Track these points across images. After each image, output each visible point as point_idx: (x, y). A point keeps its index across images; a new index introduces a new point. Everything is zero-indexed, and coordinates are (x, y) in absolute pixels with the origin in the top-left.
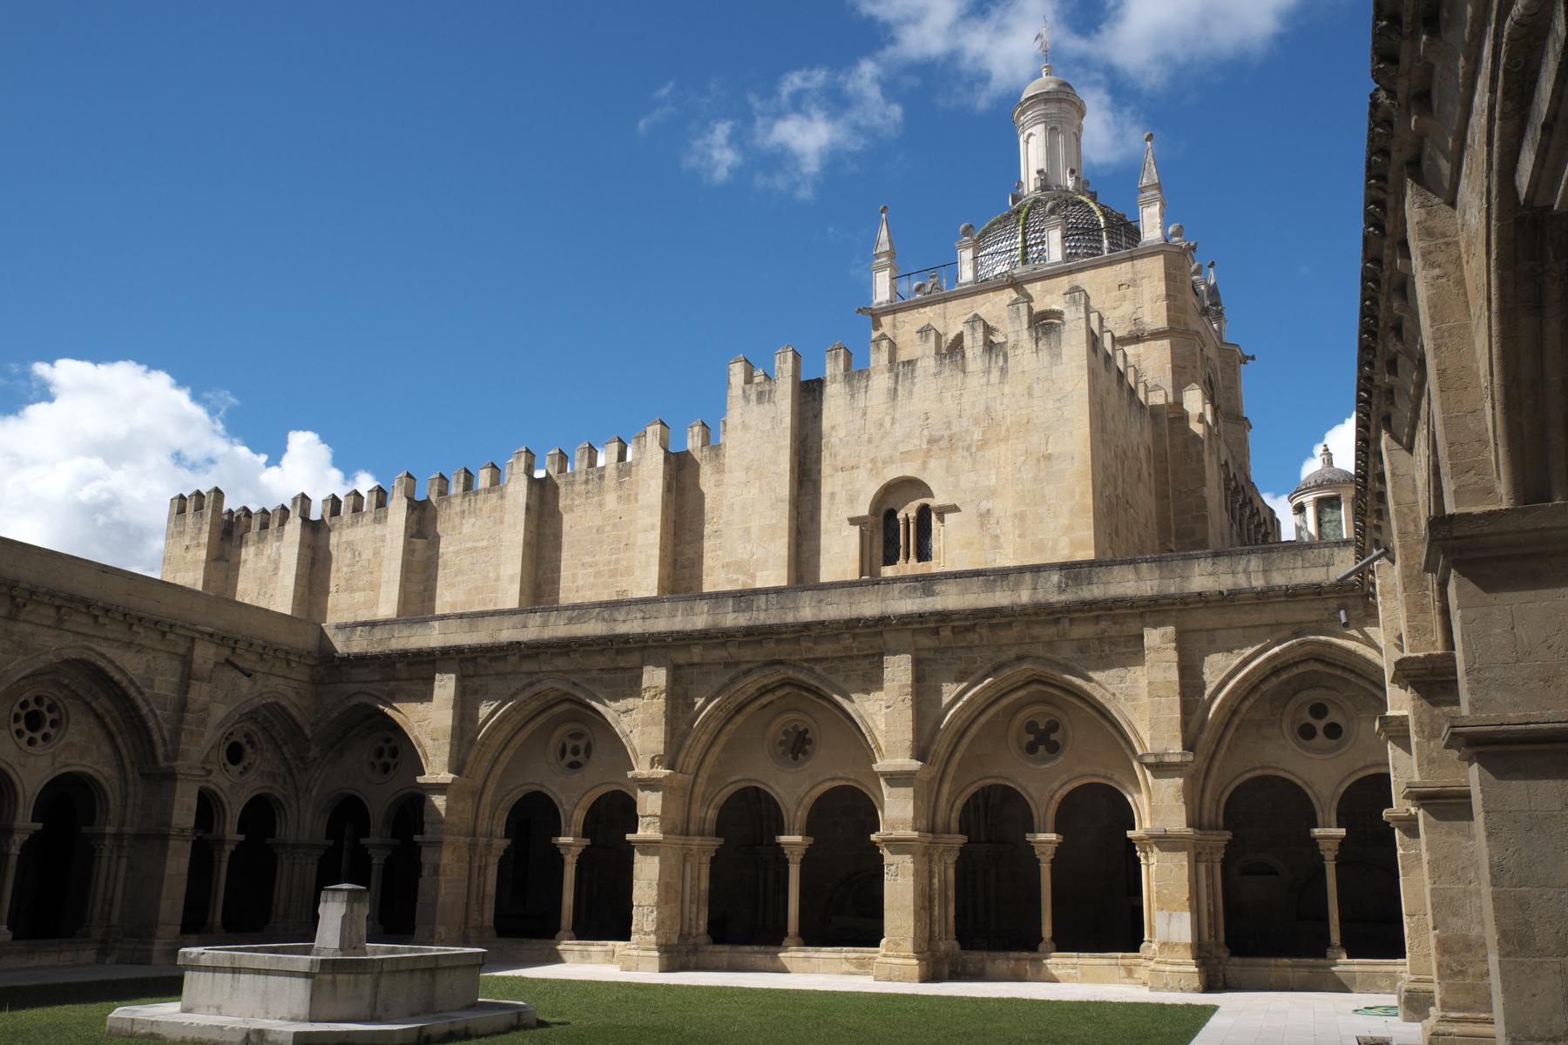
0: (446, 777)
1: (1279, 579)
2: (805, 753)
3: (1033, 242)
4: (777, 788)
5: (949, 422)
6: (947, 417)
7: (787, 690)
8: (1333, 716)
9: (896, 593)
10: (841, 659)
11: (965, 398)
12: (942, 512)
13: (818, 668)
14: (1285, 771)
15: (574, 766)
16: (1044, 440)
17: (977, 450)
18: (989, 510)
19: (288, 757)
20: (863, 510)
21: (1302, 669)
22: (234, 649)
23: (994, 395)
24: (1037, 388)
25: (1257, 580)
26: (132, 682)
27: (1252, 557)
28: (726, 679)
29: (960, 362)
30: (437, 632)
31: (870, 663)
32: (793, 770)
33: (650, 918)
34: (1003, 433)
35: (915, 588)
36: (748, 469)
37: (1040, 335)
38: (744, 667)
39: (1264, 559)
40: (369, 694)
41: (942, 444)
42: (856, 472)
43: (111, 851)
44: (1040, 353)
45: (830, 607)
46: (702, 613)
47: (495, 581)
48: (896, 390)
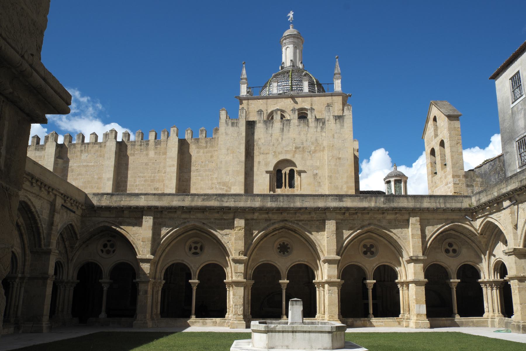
0: (149, 256)
1: (448, 206)
2: (280, 252)
3: (294, 84)
4: (279, 264)
5: (303, 142)
6: (302, 140)
7: (283, 230)
8: (455, 247)
9: (330, 200)
10: (309, 221)
11: (308, 135)
12: (300, 173)
13: (300, 223)
14: (443, 262)
15: (195, 254)
16: (338, 153)
17: (313, 153)
18: (317, 174)
19: (67, 246)
20: (271, 169)
21: (449, 232)
22: (65, 201)
23: (319, 135)
24: (336, 136)
25: (442, 205)
26: (37, 212)
27: (441, 198)
28: (266, 225)
29: (307, 123)
30: (143, 200)
31: (319, 223)
32: (285, 258)
33: (240, 309)
34: (322, 148)
35: (336, 199)
36: (228, 149)
37: (337, 118)
38: (272, 221)
39: (444, 199)
40: (109, 222)
41: (300, 149)
42: (268, 155)
43: (18, 284)
44: (337, 124)
45: (307, 203)
46: (258, 201)
47: (97, 179)
48: (283, 129)
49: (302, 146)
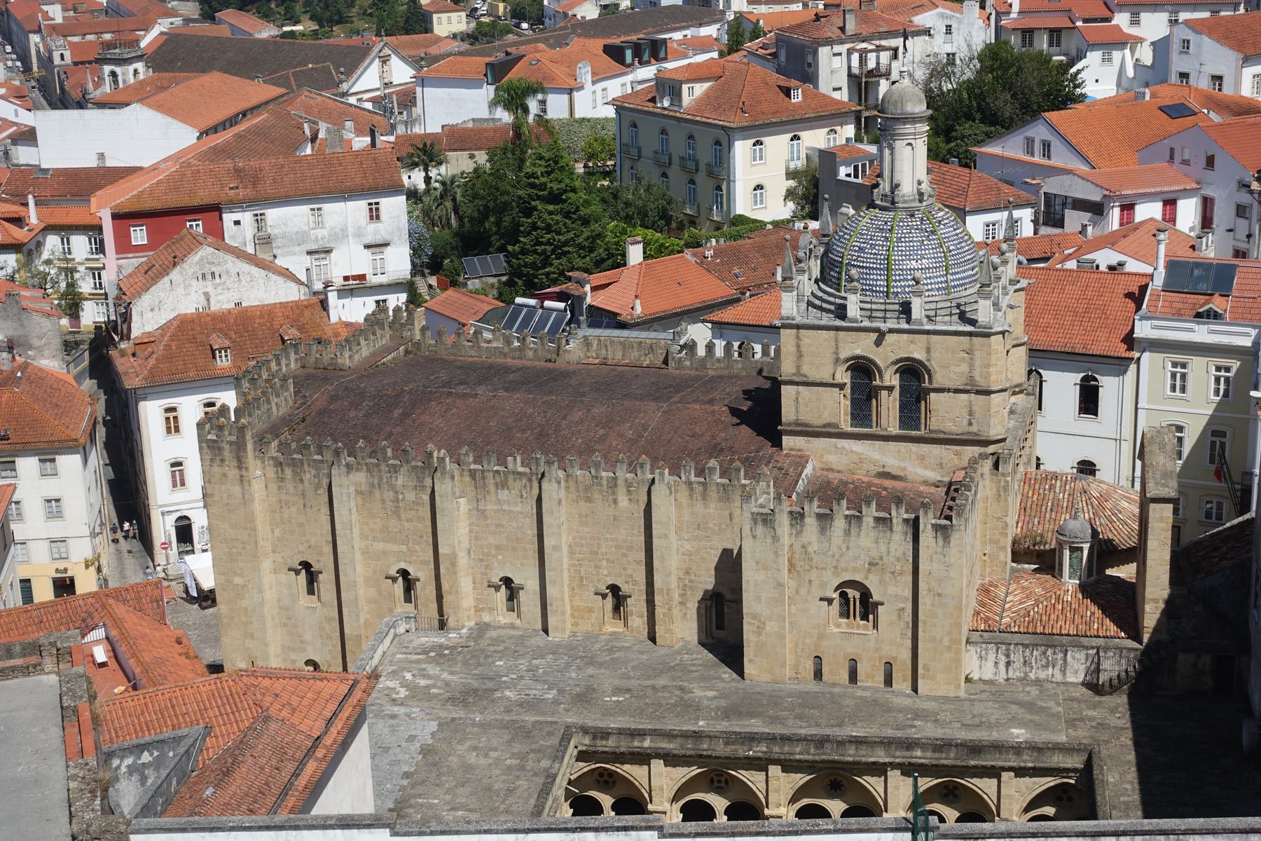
36: (758, 563)
42: (824, 572)
48: (849, 530)
49: (880, 562)
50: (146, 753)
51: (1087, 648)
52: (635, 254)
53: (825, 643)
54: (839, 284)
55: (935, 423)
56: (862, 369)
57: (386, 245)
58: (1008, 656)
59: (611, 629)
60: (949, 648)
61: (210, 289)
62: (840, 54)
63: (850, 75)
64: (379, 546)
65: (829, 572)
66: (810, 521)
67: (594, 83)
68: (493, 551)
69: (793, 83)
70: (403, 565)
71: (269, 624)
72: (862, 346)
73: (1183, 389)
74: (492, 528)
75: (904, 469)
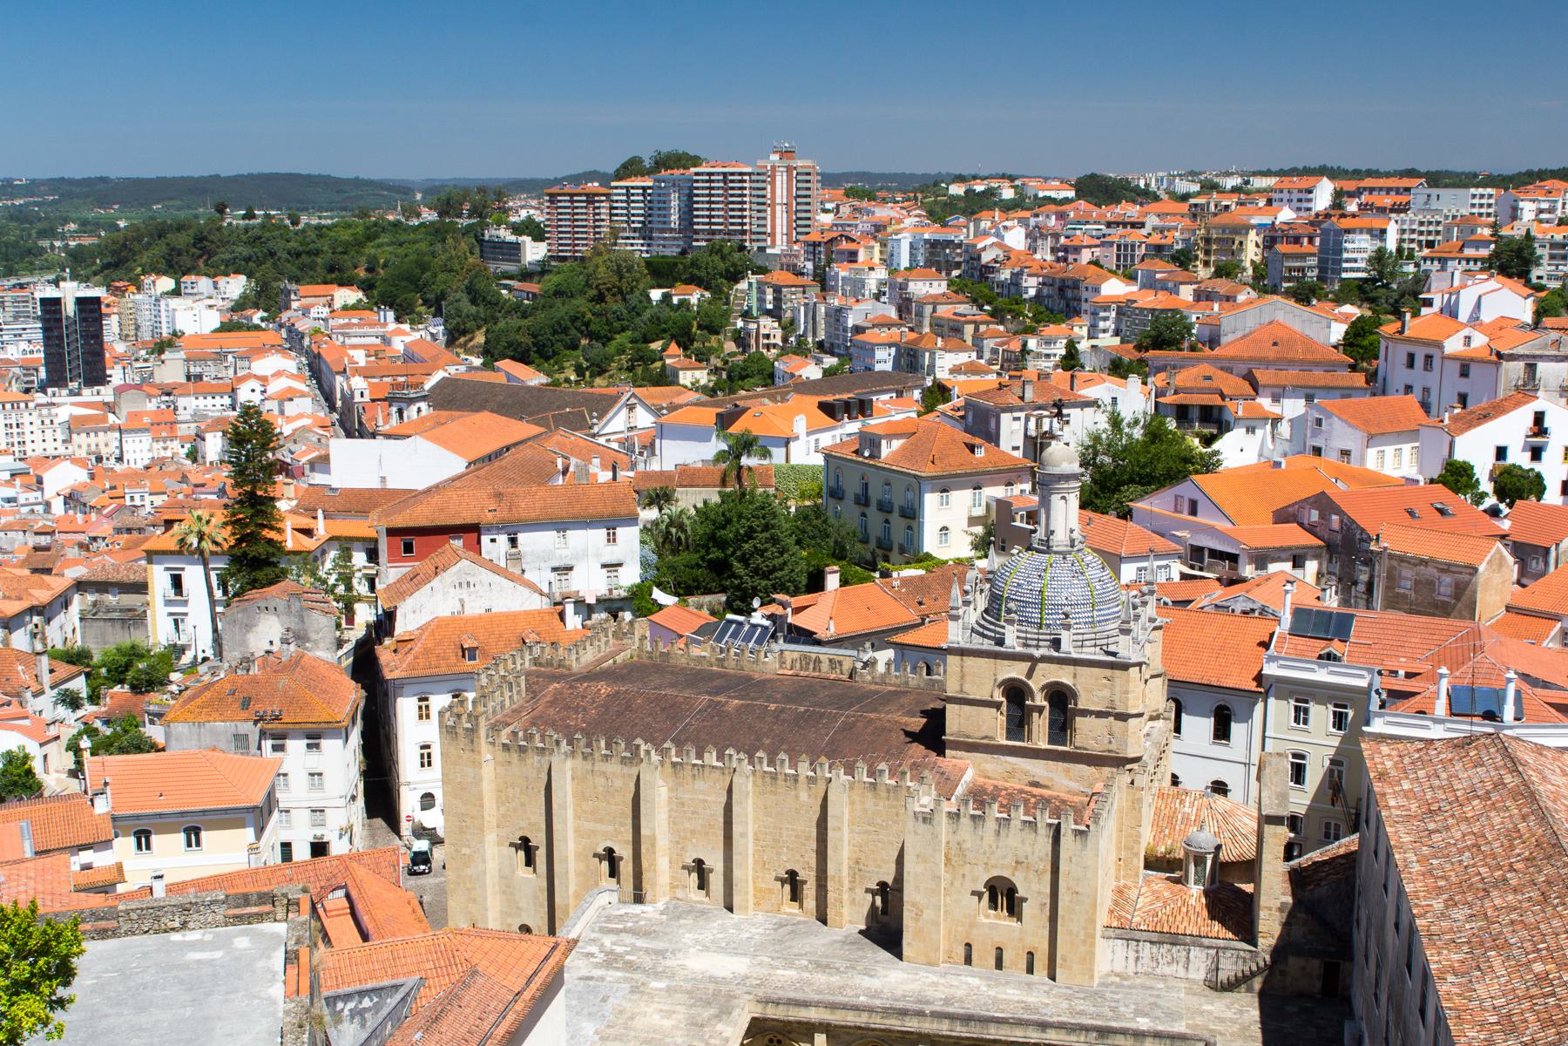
24: (1074, 860)
36: (918, 856)
50: (367, 999)
51: (1208, 947)
52: (832, 581)
53: (975, 931)
54: (1000, 615)
55: (1079, 740)
56: (1016, 693)
57: (620, 565)
58: (1137, 952)
59: (788, 910)
60: (1084, 942)
61: (465, 597)
62: (1019, 419)
63: (1026, 435)
64: (591, 825)
65: (980, 868)
66: (965, 821)
67: (808, 434)
68: (688, 835)
69: (977, 441)
70: (609, 844)
71: (489, 891)
72: (1017, 671)
73: (1305, 722)
74: (688, 815)
75: (1052, 779)
